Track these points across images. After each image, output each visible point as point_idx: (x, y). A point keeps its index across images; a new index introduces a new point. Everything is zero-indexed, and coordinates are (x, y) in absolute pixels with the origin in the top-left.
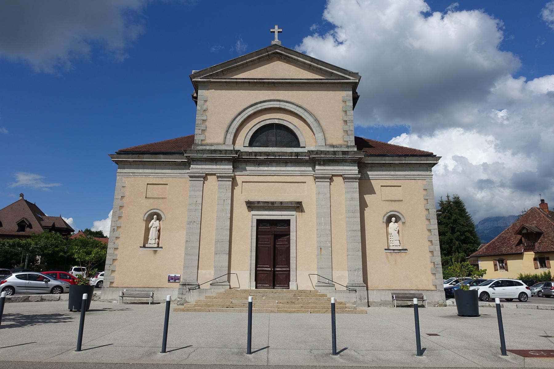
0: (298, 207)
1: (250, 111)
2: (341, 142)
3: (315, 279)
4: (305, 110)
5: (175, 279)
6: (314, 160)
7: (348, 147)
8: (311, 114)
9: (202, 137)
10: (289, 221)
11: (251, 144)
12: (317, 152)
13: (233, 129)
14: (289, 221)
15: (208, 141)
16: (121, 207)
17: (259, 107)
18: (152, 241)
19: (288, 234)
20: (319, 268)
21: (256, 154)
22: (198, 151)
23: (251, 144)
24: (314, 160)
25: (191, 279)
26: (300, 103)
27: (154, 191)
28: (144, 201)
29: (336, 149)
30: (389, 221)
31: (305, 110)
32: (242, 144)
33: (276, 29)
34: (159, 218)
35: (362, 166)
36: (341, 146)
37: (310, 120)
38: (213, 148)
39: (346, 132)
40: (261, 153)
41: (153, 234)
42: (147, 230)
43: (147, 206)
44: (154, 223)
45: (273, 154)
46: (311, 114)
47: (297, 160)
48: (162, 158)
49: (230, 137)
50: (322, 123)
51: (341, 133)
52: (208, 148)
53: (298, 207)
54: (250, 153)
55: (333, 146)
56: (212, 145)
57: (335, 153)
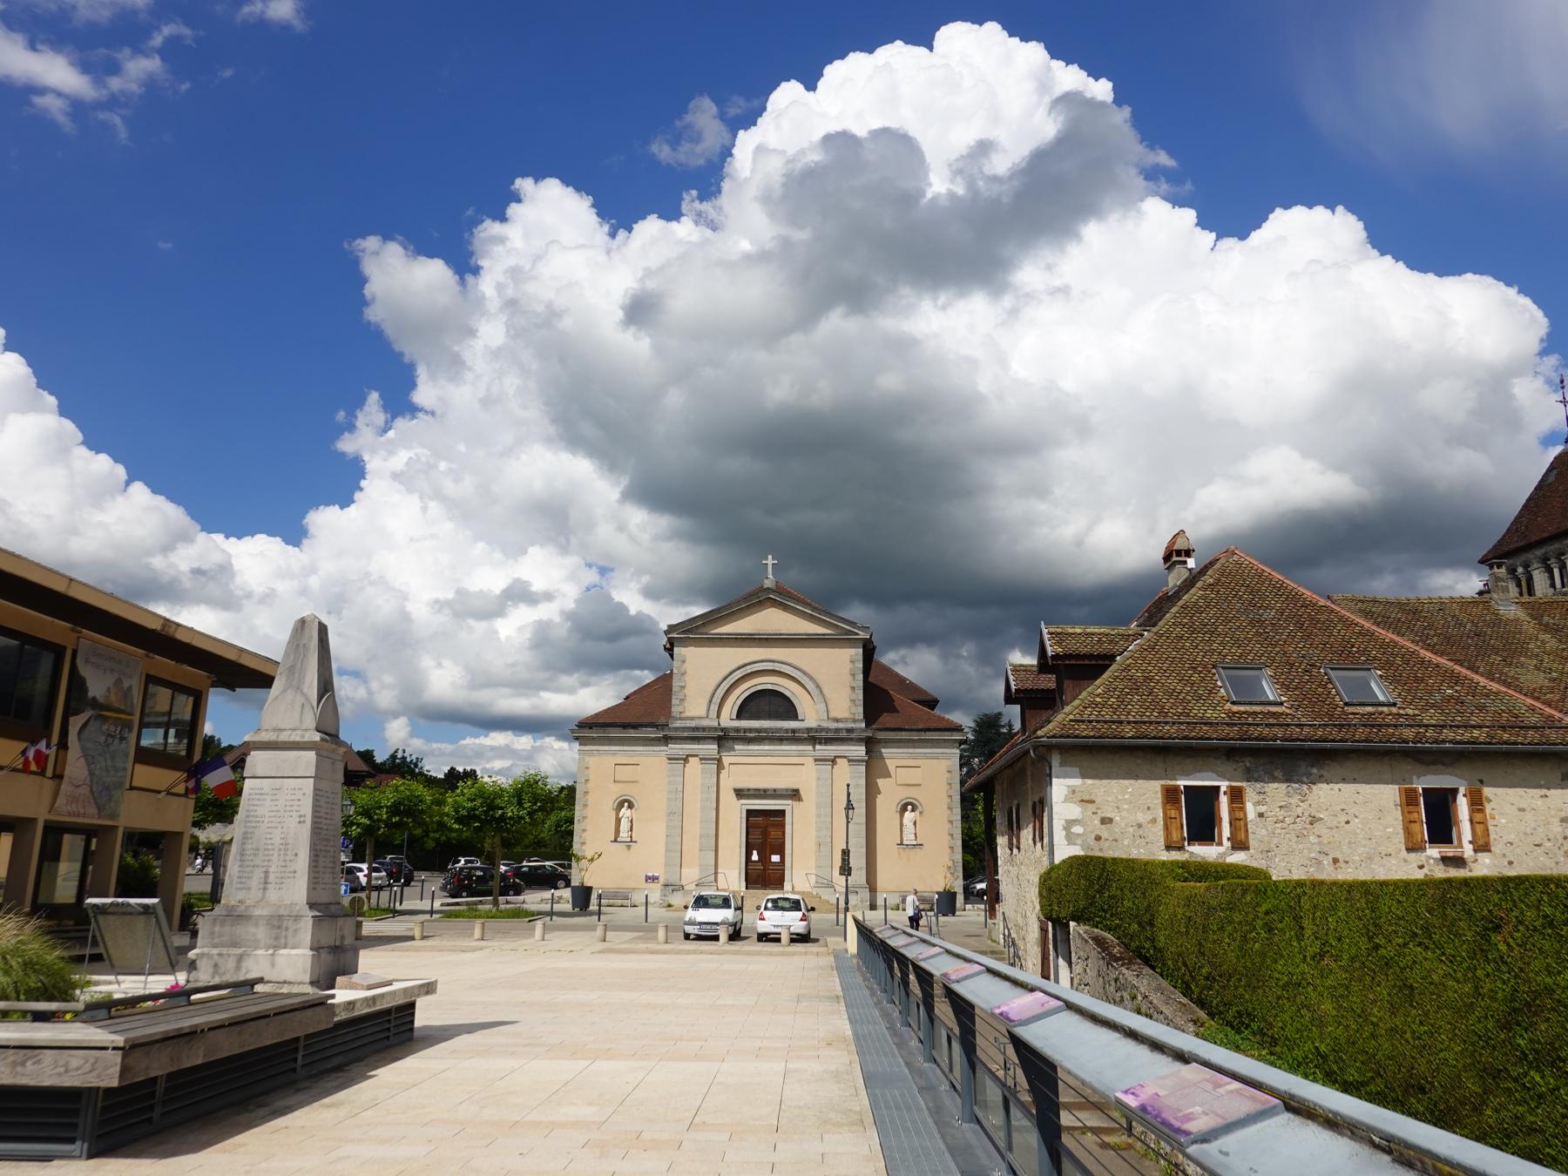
0: (795, 795)
1: (738, 675)
2: (846, 715)
3: (813, 879)
4: (805, 673)
5: (654, 879)
6: (814, 737)
7: (854, 721)
8: (811, 678)
9: (680, 709)
10: (783, 812)
11: (739, 716)
12: (817, 730)
13: (717, 699)
14: (783, 812)
15: (688, 714)
16: (586, 793)
17: (749, 669)
18: (624, 835)
19: (783, 825)
20: (818, 867)
21: (745, 730)
22: (676, 729)
23: (739, 716)
24: (814, 737)
25: (674, 879)
26: (798, 664)
27: (624, 773)
28: (612, 785)
29: (841, 725)
30: (904, 809)
31: (805, 673)
32: (728, 719)
33: (770, 561)
34: (631, 806)
35: (870, 744)
36: (846, 720)
37: (810, 686)
38: (693, 724)
39: (853, 701)
40: (751, 730)
41: (624, 825)
42: (618, 821)
43: (617, 791)
44: (624, 811)
45: (765, 730)
46: (811, 678)
47: (793, 738)
48: (632, 733)
49: (714, 708)
50: (825, 690)
51: (847, 704)
52: (689, 724)
53: (795, 795)
54: (737, 730)
55: (837, 720)
56: (692, 719)
57: (837, 730)
